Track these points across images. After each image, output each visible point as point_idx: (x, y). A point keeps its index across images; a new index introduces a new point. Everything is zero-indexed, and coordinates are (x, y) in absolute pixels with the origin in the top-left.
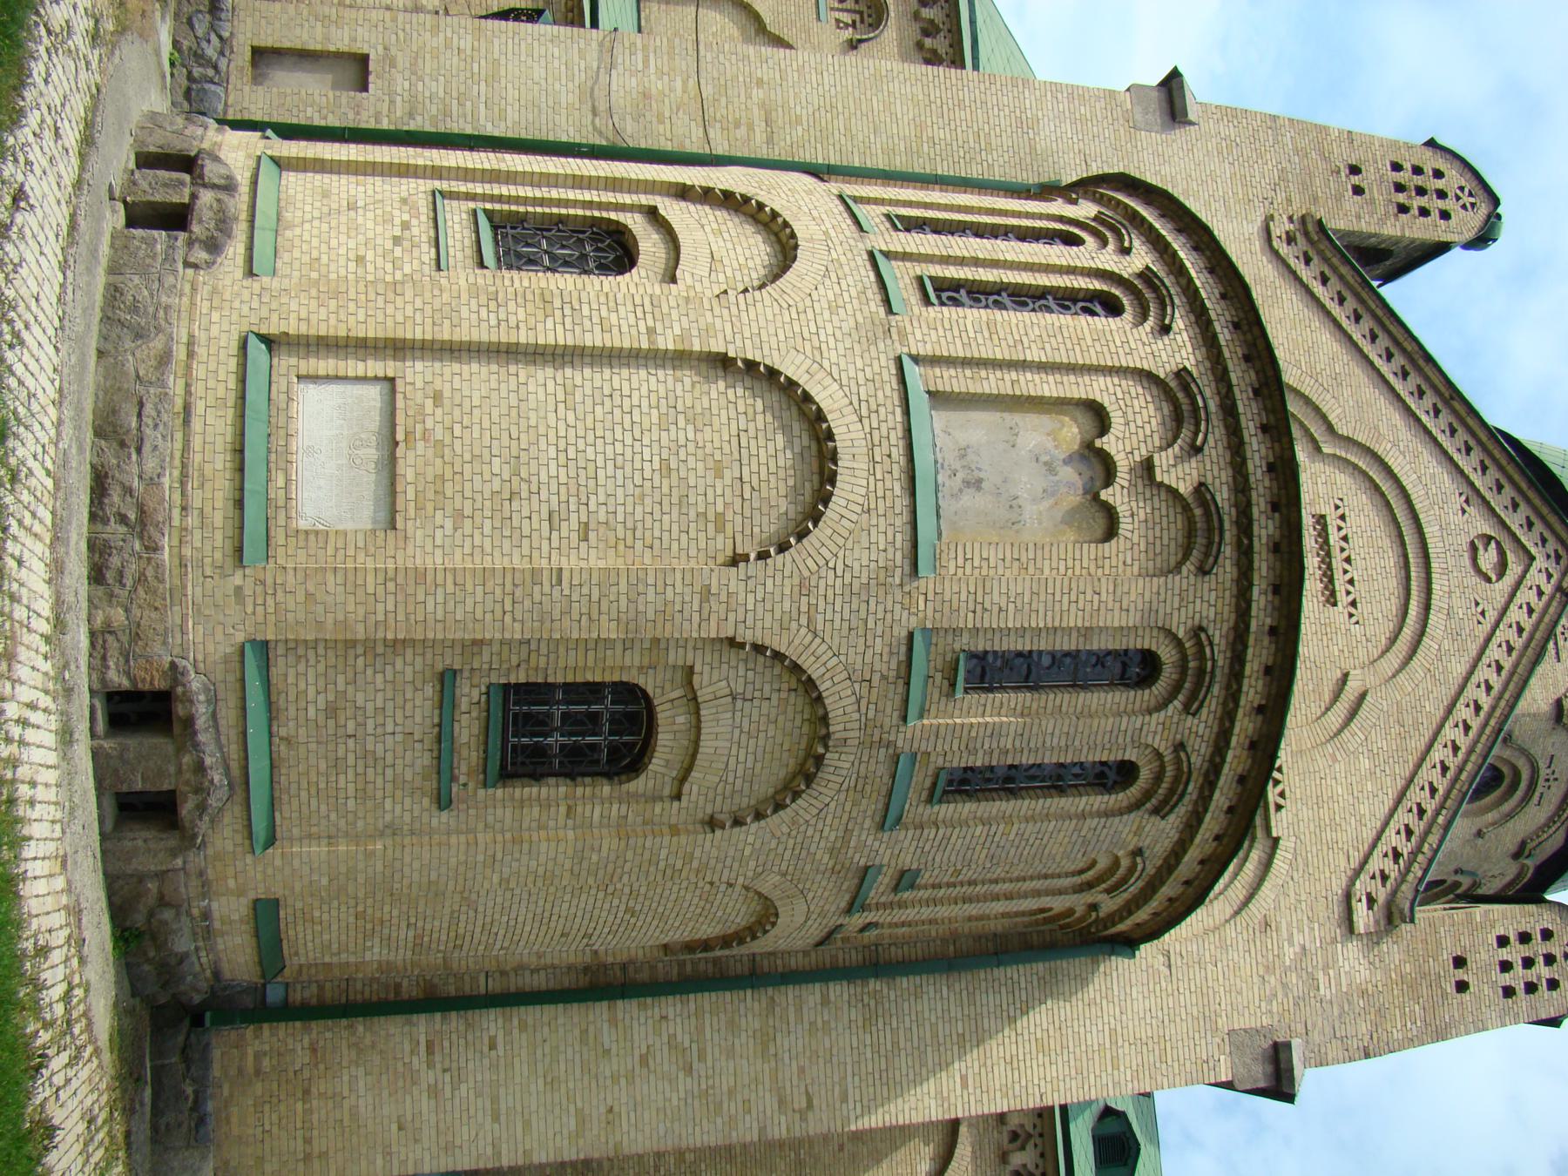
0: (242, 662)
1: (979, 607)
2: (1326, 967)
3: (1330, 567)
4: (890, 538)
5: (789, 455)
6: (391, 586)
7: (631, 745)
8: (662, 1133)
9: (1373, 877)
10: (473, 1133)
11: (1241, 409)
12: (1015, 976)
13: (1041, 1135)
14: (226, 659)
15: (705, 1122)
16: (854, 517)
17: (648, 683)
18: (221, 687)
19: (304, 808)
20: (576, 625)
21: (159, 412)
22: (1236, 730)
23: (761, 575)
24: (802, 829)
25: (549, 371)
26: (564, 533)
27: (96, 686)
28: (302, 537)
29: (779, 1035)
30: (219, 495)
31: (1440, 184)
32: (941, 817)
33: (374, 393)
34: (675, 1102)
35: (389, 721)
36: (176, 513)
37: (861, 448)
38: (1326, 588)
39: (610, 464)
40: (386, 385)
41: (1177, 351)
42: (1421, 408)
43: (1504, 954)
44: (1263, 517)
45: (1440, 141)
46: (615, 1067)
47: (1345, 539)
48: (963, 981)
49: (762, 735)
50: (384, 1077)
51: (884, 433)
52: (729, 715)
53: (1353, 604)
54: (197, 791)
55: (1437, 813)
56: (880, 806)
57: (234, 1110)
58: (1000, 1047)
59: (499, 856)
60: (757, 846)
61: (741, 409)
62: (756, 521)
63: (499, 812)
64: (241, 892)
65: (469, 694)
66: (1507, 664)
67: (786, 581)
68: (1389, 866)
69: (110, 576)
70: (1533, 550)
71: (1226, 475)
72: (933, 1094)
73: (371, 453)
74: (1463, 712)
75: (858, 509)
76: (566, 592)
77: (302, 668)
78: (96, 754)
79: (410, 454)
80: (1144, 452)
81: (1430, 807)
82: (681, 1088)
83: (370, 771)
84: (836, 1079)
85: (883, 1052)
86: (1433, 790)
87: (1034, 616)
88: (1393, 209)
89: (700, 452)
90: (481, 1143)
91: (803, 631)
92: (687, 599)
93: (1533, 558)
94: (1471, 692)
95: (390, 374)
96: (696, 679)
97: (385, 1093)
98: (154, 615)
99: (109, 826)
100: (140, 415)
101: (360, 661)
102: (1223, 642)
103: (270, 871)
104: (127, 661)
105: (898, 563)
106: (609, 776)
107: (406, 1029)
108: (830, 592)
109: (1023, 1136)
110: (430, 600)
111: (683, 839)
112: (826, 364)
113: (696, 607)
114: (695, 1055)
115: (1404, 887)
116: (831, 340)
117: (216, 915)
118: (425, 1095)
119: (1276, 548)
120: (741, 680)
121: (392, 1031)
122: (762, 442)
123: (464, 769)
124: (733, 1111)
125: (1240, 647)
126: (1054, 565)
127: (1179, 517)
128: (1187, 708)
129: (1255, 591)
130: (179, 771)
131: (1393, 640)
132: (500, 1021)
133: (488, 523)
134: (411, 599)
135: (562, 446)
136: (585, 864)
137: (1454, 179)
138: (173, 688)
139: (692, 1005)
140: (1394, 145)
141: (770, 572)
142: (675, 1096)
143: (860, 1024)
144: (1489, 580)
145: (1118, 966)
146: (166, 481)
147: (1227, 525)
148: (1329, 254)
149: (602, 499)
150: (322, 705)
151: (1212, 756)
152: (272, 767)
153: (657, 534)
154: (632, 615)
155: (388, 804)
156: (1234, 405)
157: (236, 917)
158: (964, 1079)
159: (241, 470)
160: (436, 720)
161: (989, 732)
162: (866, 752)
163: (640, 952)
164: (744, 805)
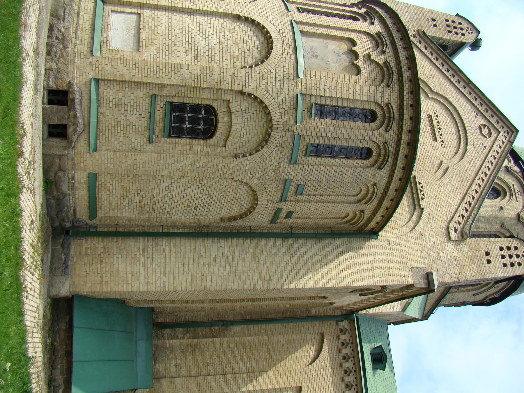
0: (91, 85)
1: (318, 89)
2: (442, 250)
3: (434, 130)
4: (290, 66)
5: (258, 42)
6: (137, 65)
7: (210, 130)
8: (220, 284)
9: (456, 223)
10: (157, 279)
11: (397, 43)
12: (338, 243)
13: (352, 343)
14: (86, 84)
15: (235, 281)
16: (278, 59)
18: (83, 92)
19: (107, 139)
20: (193, 82)
21: (70, 12)
22: (403, 138)
23: (250, 72)
24: (265, 160)
25: (186, 16)
26: (190, 57)
27: (46, 86)
28: (111, 51)
29: (259, 255)
30: (87, 36)
31: (461, 26)
32: (311, 199)
33: (134, 17)
34: (225, 274)
35: (135, 110)
36: (73, 39)
37: (280, 41)
38: (432, 133)
39: (204, 40)
40: (138, 16)
41: (376, 28)
42: (460, 86)
43: (502, 253)
44: (406, 71)
45: (460, 14)
46: (205, 261)
47: (438, 122)
48: (321, 243)
49: (251, 126)
50: (128, 258)
51: (287, 37)
52: (241, 117)
53: (442, 141)
54: (74, 124)
55: (475, 204)
56: (290, 154)
57: (78, 265)
58: (334, 265)
59: (168, 161)
60: (250, 166)
61: (244, 29)
62: (249, 58)
63: (168, 146)
65: (160, 104)
66: (494, 162)
67: (258, 75)
68: (460, 219)
69: (52, 53)
70: (499, 130)
71: (393, 60)
72: (312, 279)
73: (133, 32)
74: (481, 175)
75: (280, 57)
76: (191, 71)
77: (108, 90)
78: (43, 109)
79: (144, 32)
80: (367, 52)
81: (473, 203)
82: (227, 270)
83: (128, 127)
84: (279, 271)
85: (294, 263)
86: (473, 198)
87: (335, 93)
88: (446, 32)
89: (231, 39)
90: (159, 283)
91: (264, 90)
92: (228, 77)
93: (500, 132)
94: (483, 169)
95: (139, 12)
96: (230, 104)
97: (128, 264)
98: (65, 66)
99: (45, 137)
100: (64, 12)
101: (127, 89)
102: (396, 109)
103: (95, 161)
104: (56, 80)
105: (292, 72)
106: (203, 139)
107: (135, 244)
108: (272, 79)
109: (346, 344)
110: (149, 70)
111: (227, 160)
112: (269, 20)
113: (230, 80)
114: (231, 259)
115: (466, 226)
116: (271, 15)
117: (76, 179)
118: (141, 265)
119: (410, 80)
120: (244, 106)
121: (131, 244)
122: (250, 38)
123: (157, 130)
124: (244, 279)
125: (401, 110)
126: (341, 80)
127: (379, 71)
128: (386, 129)
129: (405, 92)
130: (69, 118)
131: (456, 153)
132: (167, 243)
133: (167, 52)
134: (143, 70)
135: (190, 33)
136: (195, 167)
137: (465, 25)
138: (69, 89)
139: (230, 243)
140: (446, 15)
141: (253, 72)
142: (225, 272)
143: (287, 254)
144: (486, 138)
145: (373, 242)
146: (71, 29)
147: (394, 74)
148: (427, 41)
149: (202, 48)
150: (114, 103)
151: (396, 148)
152: (97, 123)
153: (218, 59)
154: (210, 80)
156: (395, 42)
157: (82, 181)
158: (322, 275)
159: (94, 30)
160: (149, 111)
161: (323, 130)
162: (284, 133)
163: (213, 220)
164: (246, 151)
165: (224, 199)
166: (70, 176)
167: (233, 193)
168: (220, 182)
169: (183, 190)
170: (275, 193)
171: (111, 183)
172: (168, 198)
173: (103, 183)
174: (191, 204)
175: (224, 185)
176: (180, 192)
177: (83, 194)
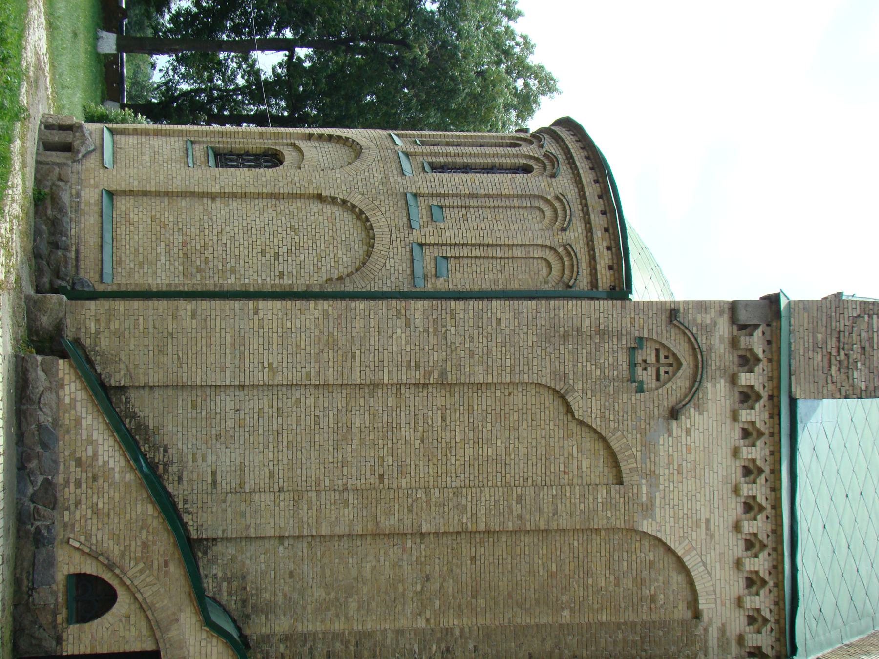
64: (96, 186)
103: (110, 176)
136: (260, 182)
155: (165, 165)
157: (92, 201)
165: (318, 235)
166: (74, 191)
167: (330, 225)
168: (303, 207)
169: (249, 221)
170: (396, 213)
171: (136, 212)
172: (228, 237)
173: (123, 214)
174: (268, 248)
175: (312, 211)
176: (245, 225)
177: (92, 221)
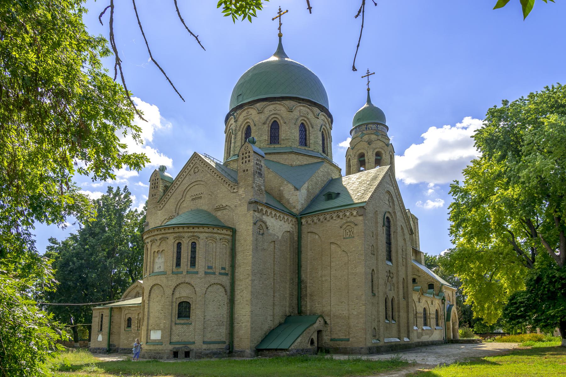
17: (178, 303)
65: (178, 321)
